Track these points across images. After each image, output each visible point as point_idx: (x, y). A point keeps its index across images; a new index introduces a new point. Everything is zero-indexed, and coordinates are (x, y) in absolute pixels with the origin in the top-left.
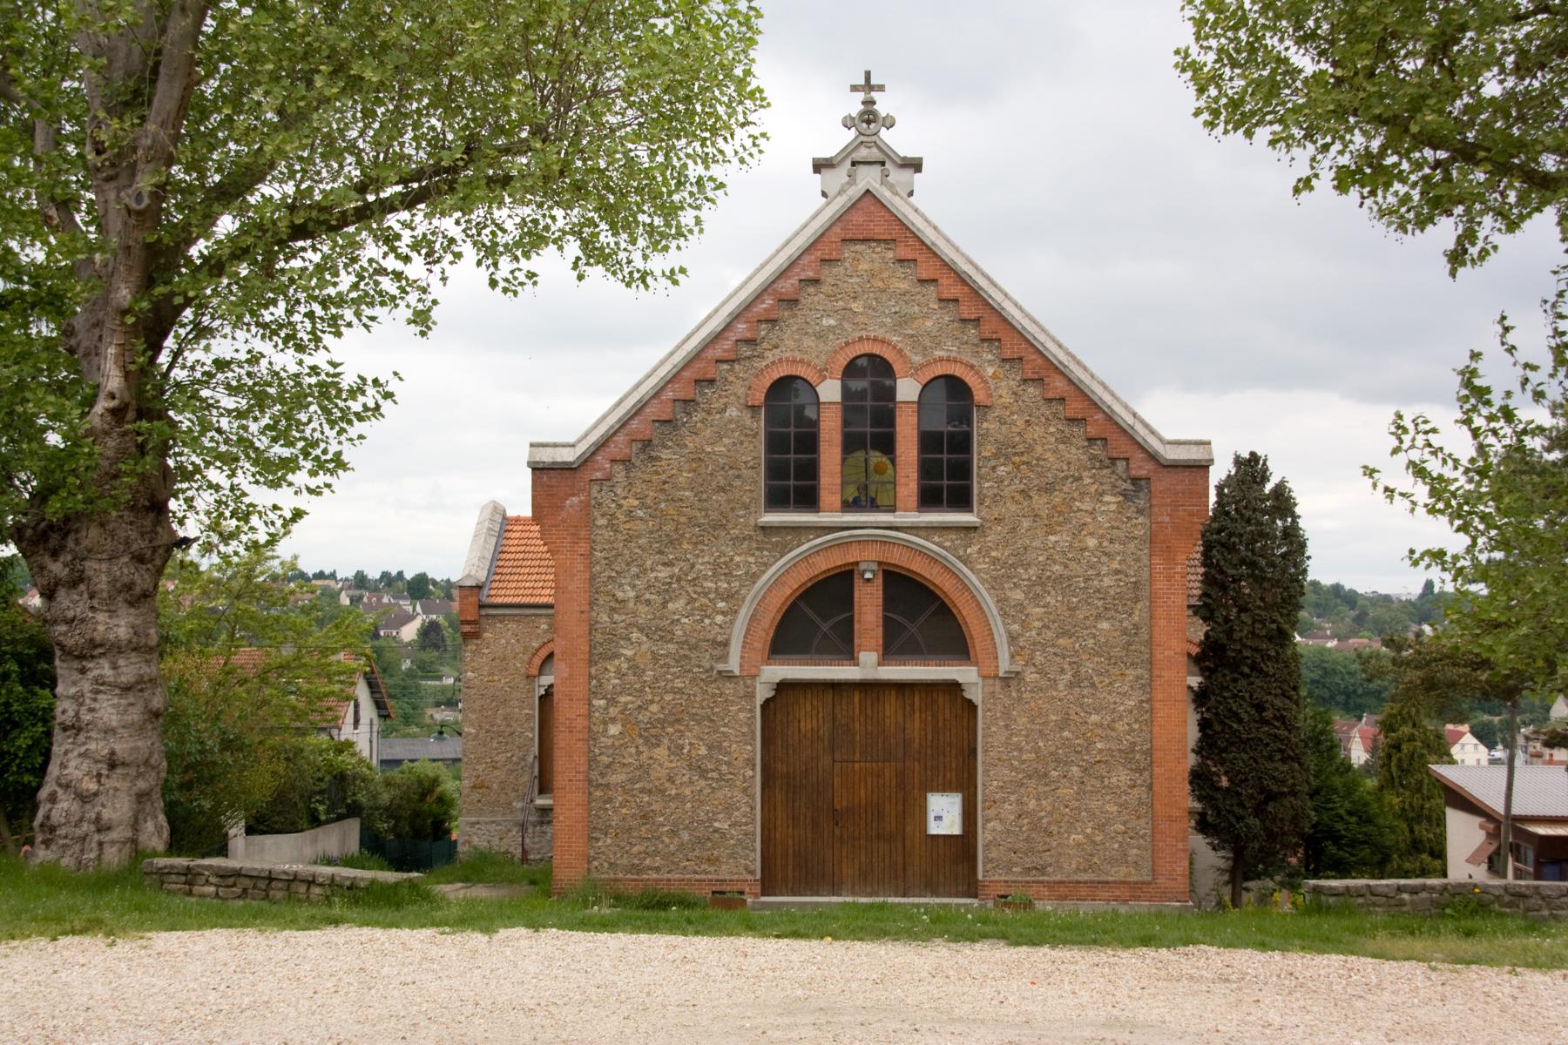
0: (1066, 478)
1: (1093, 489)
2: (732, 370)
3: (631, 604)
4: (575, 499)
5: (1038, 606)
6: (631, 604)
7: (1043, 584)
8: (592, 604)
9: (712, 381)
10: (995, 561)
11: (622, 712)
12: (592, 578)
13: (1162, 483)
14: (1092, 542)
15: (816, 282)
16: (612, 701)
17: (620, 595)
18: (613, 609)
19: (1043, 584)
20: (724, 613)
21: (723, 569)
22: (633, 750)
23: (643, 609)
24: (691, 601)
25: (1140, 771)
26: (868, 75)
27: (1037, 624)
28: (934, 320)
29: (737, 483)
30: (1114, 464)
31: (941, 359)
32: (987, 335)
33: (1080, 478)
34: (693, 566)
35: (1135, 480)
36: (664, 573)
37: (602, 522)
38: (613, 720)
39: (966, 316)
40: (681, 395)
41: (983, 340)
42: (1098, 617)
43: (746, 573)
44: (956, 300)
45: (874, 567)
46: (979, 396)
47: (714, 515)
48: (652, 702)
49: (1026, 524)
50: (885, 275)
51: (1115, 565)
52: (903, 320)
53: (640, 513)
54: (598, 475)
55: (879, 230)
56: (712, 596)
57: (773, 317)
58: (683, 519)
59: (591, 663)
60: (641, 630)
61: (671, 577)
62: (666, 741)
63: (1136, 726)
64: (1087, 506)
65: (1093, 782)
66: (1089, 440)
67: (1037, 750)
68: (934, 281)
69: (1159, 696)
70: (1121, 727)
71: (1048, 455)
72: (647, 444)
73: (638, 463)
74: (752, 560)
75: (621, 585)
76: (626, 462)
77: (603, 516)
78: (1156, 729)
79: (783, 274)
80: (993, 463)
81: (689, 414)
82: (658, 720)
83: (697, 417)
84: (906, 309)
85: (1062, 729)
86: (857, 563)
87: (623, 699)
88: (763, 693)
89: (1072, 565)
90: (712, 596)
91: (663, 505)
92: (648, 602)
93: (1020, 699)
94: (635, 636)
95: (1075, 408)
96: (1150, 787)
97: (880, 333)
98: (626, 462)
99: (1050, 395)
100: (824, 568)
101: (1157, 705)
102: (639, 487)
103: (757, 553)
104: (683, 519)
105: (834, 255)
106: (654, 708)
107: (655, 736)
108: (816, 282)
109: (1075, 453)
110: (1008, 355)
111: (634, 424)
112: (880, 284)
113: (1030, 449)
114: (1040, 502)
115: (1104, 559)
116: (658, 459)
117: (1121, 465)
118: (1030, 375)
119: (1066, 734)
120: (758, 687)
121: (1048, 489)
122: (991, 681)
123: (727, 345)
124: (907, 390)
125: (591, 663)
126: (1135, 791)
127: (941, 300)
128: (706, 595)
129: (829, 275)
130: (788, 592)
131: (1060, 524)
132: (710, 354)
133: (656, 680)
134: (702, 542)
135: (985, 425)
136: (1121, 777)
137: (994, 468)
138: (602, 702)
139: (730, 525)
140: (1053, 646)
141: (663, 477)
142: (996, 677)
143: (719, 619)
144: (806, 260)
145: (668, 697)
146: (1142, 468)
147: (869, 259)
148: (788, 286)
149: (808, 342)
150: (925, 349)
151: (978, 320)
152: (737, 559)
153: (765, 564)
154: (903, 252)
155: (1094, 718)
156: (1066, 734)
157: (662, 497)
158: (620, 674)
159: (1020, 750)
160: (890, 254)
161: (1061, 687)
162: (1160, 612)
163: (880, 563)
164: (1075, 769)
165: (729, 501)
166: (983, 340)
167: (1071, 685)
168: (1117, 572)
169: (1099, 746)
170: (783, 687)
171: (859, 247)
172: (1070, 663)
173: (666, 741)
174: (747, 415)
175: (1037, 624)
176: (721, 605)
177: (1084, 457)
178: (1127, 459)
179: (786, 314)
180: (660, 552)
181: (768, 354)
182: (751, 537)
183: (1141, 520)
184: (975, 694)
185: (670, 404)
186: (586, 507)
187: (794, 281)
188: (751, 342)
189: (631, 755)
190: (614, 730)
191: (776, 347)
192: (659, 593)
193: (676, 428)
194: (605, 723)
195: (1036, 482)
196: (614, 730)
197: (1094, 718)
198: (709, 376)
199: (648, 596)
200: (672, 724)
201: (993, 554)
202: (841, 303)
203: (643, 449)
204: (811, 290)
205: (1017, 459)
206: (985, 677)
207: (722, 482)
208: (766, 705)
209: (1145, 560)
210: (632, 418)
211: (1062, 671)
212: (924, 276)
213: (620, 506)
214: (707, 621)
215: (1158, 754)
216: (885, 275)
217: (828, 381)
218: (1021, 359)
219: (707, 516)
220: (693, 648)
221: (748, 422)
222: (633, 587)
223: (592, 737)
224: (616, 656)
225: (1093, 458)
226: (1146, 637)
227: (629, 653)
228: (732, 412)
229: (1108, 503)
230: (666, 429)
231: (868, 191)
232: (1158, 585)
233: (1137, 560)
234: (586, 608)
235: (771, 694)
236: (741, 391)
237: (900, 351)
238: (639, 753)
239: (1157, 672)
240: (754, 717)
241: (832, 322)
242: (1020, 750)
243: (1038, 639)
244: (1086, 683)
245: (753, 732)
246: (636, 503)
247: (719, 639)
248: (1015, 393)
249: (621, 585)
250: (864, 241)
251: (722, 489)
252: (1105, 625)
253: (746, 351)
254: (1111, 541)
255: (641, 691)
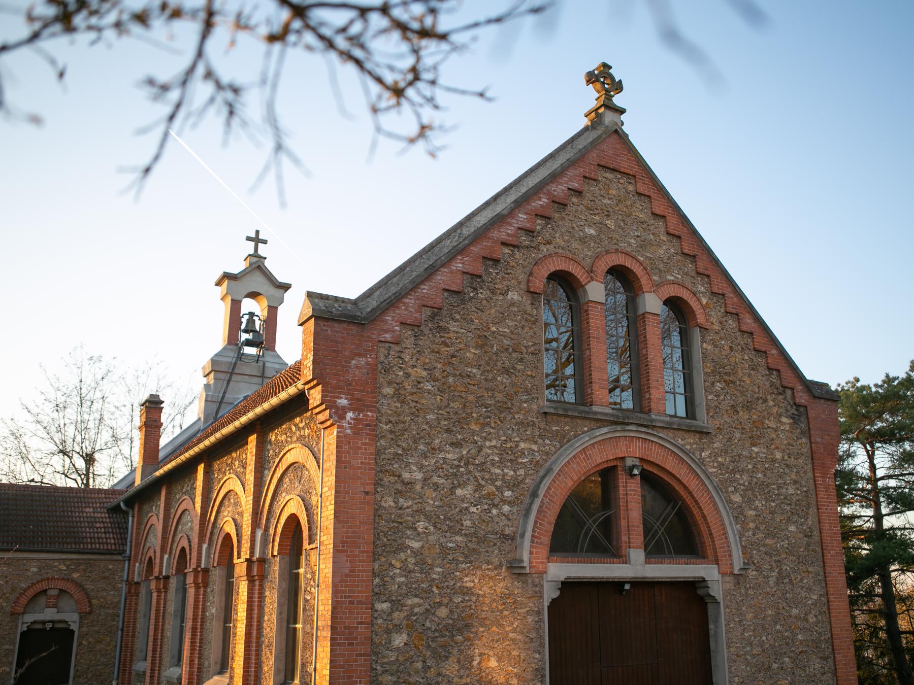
0: (758, 399)
1: (775, 410)
2: (513, 255)
3: (418, 487)
4: (362, 361)
5: (751, 509)
6: (418, 487)
7: (752, 489)
8: (378, 483)
9: (496, 261)
10: (720, 466)
11: (408, 618)
12: (378, 453)
13: (817, 410)
14: (778, 455)
15: (579, 193)
16: (397, 604)
17: (406, 476)
18: (399, 493)
19: (752, 489)
20: (510, 503)
21: (510, 456)
22: (419, 665)
23: (430, 493)
24: (479, 487)
25: (825, 659)
26: (257, 232)
27: (752, 525)
28: (665, 249)
29: (520, 367)
30: (784, 391)
31: (673, 283)
32: (701, 271)
33: (765, 401)
34: (480, 449)
35: (798, 406)
36: (451, 455)
37: (388, 391)
38: (398, 629)
39: (686, 251)
40: (470, 269)
41: (698, 273)
42: (789, 520)
43: (531, 461)
44: (679, 237)
45: (637, 462)
46: (701, 319)
47: (500, 397)
48: (440, 604)
49: (738, 435)
50: (628, 203)
51: (794, 476)
52: (644, 245)
53: (429, 387)
54: (388, 336)
55: (625, 164)
56: (499, 483)
57: (547, 214)
58: (471, 398)
59: (375, 556)
60: (428, 518)
61: (460, 459)
62: (455, 651)
63: (820, 617)
64: (773, 424)
65: (798, 672)
66: (769, 369)
67: (761, 644)
68: (664, 217)
69: (831, 591)
70: (811, 619)
71: (746, 378)
72: (436, 312)
73: (427, 331)
74: (535, 447)
75: (408, 464)
76: (415, 326)
77: (390, 383)
78: (833, 619)
79: (554, 177)
80: (711, 379)
81: (475, 289)
82: (446, 627)
83: (483, 294)
84: (644, 235)
85: (776, 623)
86: (623, 459)
87: (409, 602)
88: (550, 593)
89: (768, 473)
90: (499, 483)
91: (451, 380)
92: (436, 486)
93: (747, 595)
94: (421, 525)
95: (760, 341)
96: (835, 672)
97: (629, 249)
98: (415, 326)
99: (744, 328)
100: (599, 461)
101: (831, 598)
102: (427, 357)
103: (540, 441)
104: (471, 398)
105: (593, 176)
106: (443, 612)
107: (444, 646)
108: (579, 193)
109: (762, 379)
110: (715, 290)
111: (425, 289)
112: (625, 209)
113: (734, 372)
114: (743, 415)
115: (787, 470)
116: (446, 330)
117: (789, 392)
118: (730, 309)
119: (778, 627)
120: (545, 584)
121: (748, 407)
122: (727, 579)
123: (511, 230)
124: (652, 303)
125: (375, 556)
126: (824, 678)
127: (668, 234)
128: (493, 481)
129: (592, 190)
130: (570, 483)
131: (759, 437)
132: (495, 234)
133: (445, 577)
134: (488, 424)
135: (705, 345)
136: (816, 665)
137: (713, 384)
138: (385, 606)
139: (515, 409)
140: (764, 545)
141: (451, 350)
142: (732, 574)
143: (506, 508)
144: (571, 173)
145: (458, 599)
146: (802, 398)
147: (617, 187)
148: (559, 189)
149: (575, 245)
150: (660, 271)
151: (694, 256)
152: (522, 445)
153: (547, 453)
154: (642, 189)
155: (795, 611)
156: (778, 627)
157: (449, 369)
158: (407, 571)
159: (751, 644)
160: (631, 188)
161: (771, 583)
162: (824, 517)
163: (641, 459)
164: (787, 660)
165: (513, 384)
166: (698, 273)
167: (777, 583)
168: (795, 482)
169: (800, 637)
170: (568, 586)
171: (609, 175)
172: (777, 561)
173: (455, 651)
174: (526, 300)
175: (752, 525)
176: (507, 494)
177: (767, 384)
178: (792, 389)
179: (557, 215)
180: (448, 431)
181: (544, 248)
182: (534, 424)
183: (804, 440)
184: (717, 590)
185: (459, 276)
186: (373, 370)
187: (563, 187)
188: (530, 232)
189: (417, 672)
190: (399, 640)
191: (549, 243)
192: (447, 477)
193: (463, 301)
194: (388, 632)
195: (741, 399)
196: (399, 640)
197: (795, 611)
198: (495, 256)
199: (435, 479)
200: (460, 630)
201: (720, 459)
202: (597, 218)
203: (433, 317)
204: (575, 200)
205: (726, 378)
206: (723, 574)
207: (507, 364)
208: (554, 603)
209: (810, 474)
210: (422, 282)
211: (771, 570)
212: (658, 211)
213: (408, 375)
214: (494, 511)
215: (837, 643)
216: (628, 203)
217: (594, 283)
218: (723, 295)
219: (493, 396)
220: (482, 540)
221: (529, 308)
222: (421, 467)
223: (375, 651)
224: (403, 548)
225: (772, 385)
226: (817, 539)
227: (416, 545)
228: (513, 296)
229: (785, 424)
230: (453, 300)
231: (616, 131)
232: (821, 495)
233: (805, 473)
234: (370, 488)
235: (556, 594)
236: (522, 277)
237: (645, 269)
238: (426, 668)
239: (828, 569)
240: (541, 620)
241: (592, 232)
242: (751, 644)
243: (754, 539)
244: (787, 580)
245: (541, 637)
246: (425, 374)
247: (507, 531)
248: (721, 323)
249: (408, 464)
250: (614, 170)
251: (506, 371)
252: (792, 528)
253: (524, 240)
254: (789, 456)
255: (429, 591)
